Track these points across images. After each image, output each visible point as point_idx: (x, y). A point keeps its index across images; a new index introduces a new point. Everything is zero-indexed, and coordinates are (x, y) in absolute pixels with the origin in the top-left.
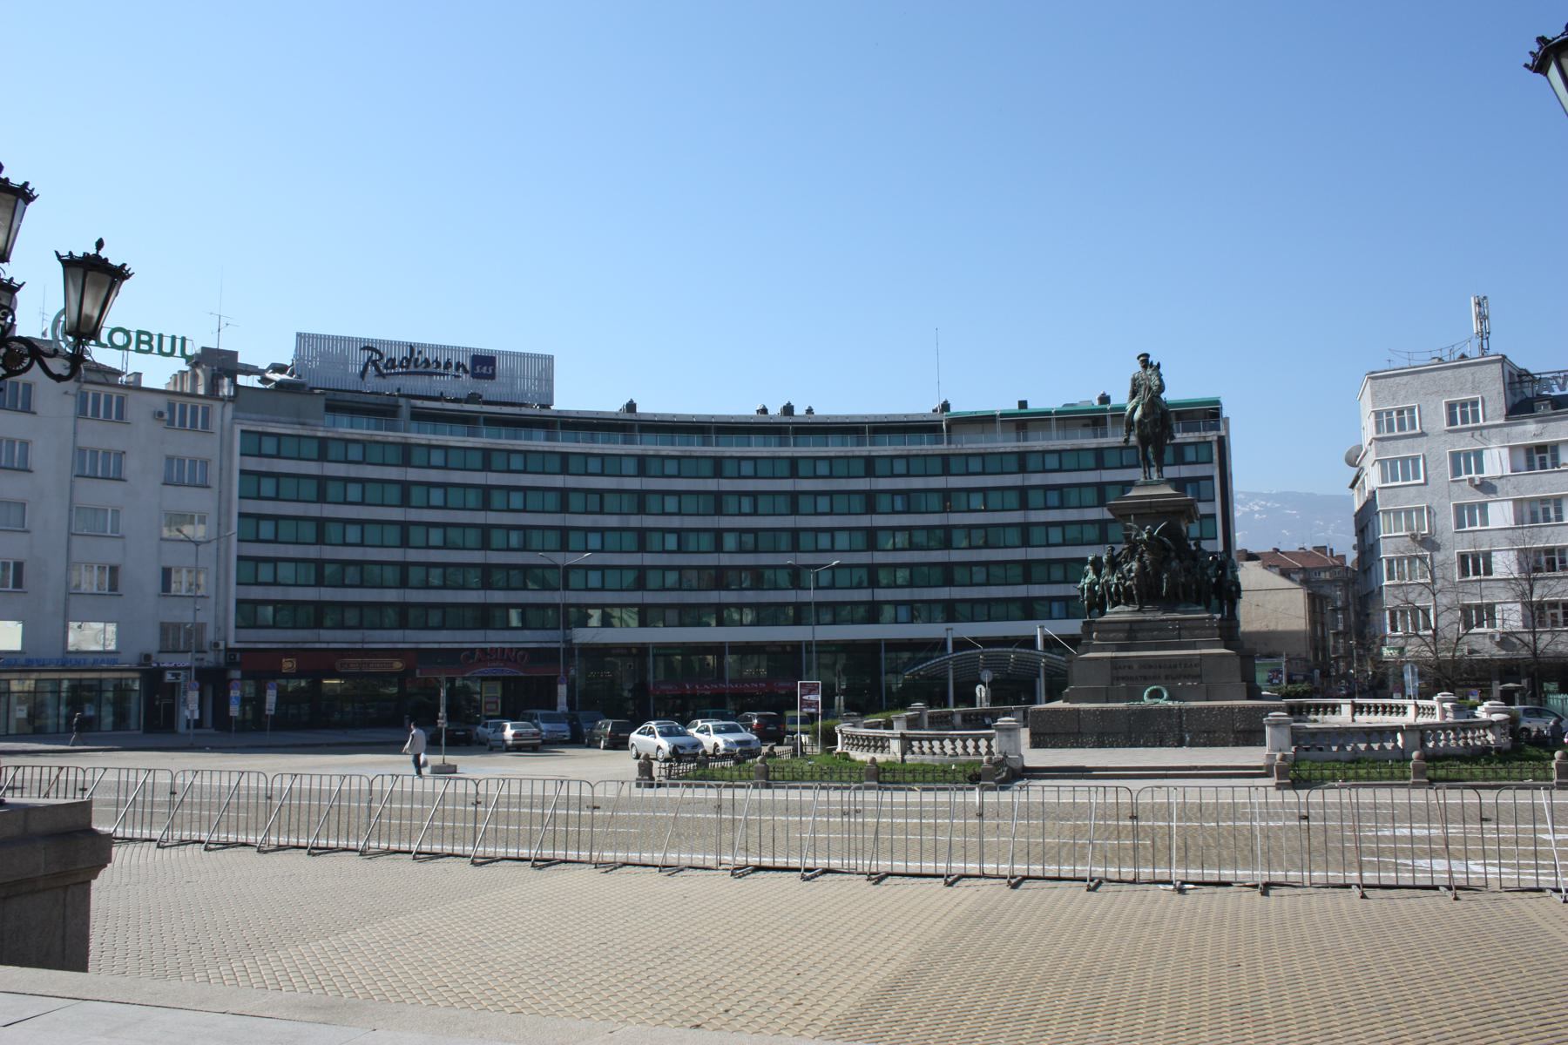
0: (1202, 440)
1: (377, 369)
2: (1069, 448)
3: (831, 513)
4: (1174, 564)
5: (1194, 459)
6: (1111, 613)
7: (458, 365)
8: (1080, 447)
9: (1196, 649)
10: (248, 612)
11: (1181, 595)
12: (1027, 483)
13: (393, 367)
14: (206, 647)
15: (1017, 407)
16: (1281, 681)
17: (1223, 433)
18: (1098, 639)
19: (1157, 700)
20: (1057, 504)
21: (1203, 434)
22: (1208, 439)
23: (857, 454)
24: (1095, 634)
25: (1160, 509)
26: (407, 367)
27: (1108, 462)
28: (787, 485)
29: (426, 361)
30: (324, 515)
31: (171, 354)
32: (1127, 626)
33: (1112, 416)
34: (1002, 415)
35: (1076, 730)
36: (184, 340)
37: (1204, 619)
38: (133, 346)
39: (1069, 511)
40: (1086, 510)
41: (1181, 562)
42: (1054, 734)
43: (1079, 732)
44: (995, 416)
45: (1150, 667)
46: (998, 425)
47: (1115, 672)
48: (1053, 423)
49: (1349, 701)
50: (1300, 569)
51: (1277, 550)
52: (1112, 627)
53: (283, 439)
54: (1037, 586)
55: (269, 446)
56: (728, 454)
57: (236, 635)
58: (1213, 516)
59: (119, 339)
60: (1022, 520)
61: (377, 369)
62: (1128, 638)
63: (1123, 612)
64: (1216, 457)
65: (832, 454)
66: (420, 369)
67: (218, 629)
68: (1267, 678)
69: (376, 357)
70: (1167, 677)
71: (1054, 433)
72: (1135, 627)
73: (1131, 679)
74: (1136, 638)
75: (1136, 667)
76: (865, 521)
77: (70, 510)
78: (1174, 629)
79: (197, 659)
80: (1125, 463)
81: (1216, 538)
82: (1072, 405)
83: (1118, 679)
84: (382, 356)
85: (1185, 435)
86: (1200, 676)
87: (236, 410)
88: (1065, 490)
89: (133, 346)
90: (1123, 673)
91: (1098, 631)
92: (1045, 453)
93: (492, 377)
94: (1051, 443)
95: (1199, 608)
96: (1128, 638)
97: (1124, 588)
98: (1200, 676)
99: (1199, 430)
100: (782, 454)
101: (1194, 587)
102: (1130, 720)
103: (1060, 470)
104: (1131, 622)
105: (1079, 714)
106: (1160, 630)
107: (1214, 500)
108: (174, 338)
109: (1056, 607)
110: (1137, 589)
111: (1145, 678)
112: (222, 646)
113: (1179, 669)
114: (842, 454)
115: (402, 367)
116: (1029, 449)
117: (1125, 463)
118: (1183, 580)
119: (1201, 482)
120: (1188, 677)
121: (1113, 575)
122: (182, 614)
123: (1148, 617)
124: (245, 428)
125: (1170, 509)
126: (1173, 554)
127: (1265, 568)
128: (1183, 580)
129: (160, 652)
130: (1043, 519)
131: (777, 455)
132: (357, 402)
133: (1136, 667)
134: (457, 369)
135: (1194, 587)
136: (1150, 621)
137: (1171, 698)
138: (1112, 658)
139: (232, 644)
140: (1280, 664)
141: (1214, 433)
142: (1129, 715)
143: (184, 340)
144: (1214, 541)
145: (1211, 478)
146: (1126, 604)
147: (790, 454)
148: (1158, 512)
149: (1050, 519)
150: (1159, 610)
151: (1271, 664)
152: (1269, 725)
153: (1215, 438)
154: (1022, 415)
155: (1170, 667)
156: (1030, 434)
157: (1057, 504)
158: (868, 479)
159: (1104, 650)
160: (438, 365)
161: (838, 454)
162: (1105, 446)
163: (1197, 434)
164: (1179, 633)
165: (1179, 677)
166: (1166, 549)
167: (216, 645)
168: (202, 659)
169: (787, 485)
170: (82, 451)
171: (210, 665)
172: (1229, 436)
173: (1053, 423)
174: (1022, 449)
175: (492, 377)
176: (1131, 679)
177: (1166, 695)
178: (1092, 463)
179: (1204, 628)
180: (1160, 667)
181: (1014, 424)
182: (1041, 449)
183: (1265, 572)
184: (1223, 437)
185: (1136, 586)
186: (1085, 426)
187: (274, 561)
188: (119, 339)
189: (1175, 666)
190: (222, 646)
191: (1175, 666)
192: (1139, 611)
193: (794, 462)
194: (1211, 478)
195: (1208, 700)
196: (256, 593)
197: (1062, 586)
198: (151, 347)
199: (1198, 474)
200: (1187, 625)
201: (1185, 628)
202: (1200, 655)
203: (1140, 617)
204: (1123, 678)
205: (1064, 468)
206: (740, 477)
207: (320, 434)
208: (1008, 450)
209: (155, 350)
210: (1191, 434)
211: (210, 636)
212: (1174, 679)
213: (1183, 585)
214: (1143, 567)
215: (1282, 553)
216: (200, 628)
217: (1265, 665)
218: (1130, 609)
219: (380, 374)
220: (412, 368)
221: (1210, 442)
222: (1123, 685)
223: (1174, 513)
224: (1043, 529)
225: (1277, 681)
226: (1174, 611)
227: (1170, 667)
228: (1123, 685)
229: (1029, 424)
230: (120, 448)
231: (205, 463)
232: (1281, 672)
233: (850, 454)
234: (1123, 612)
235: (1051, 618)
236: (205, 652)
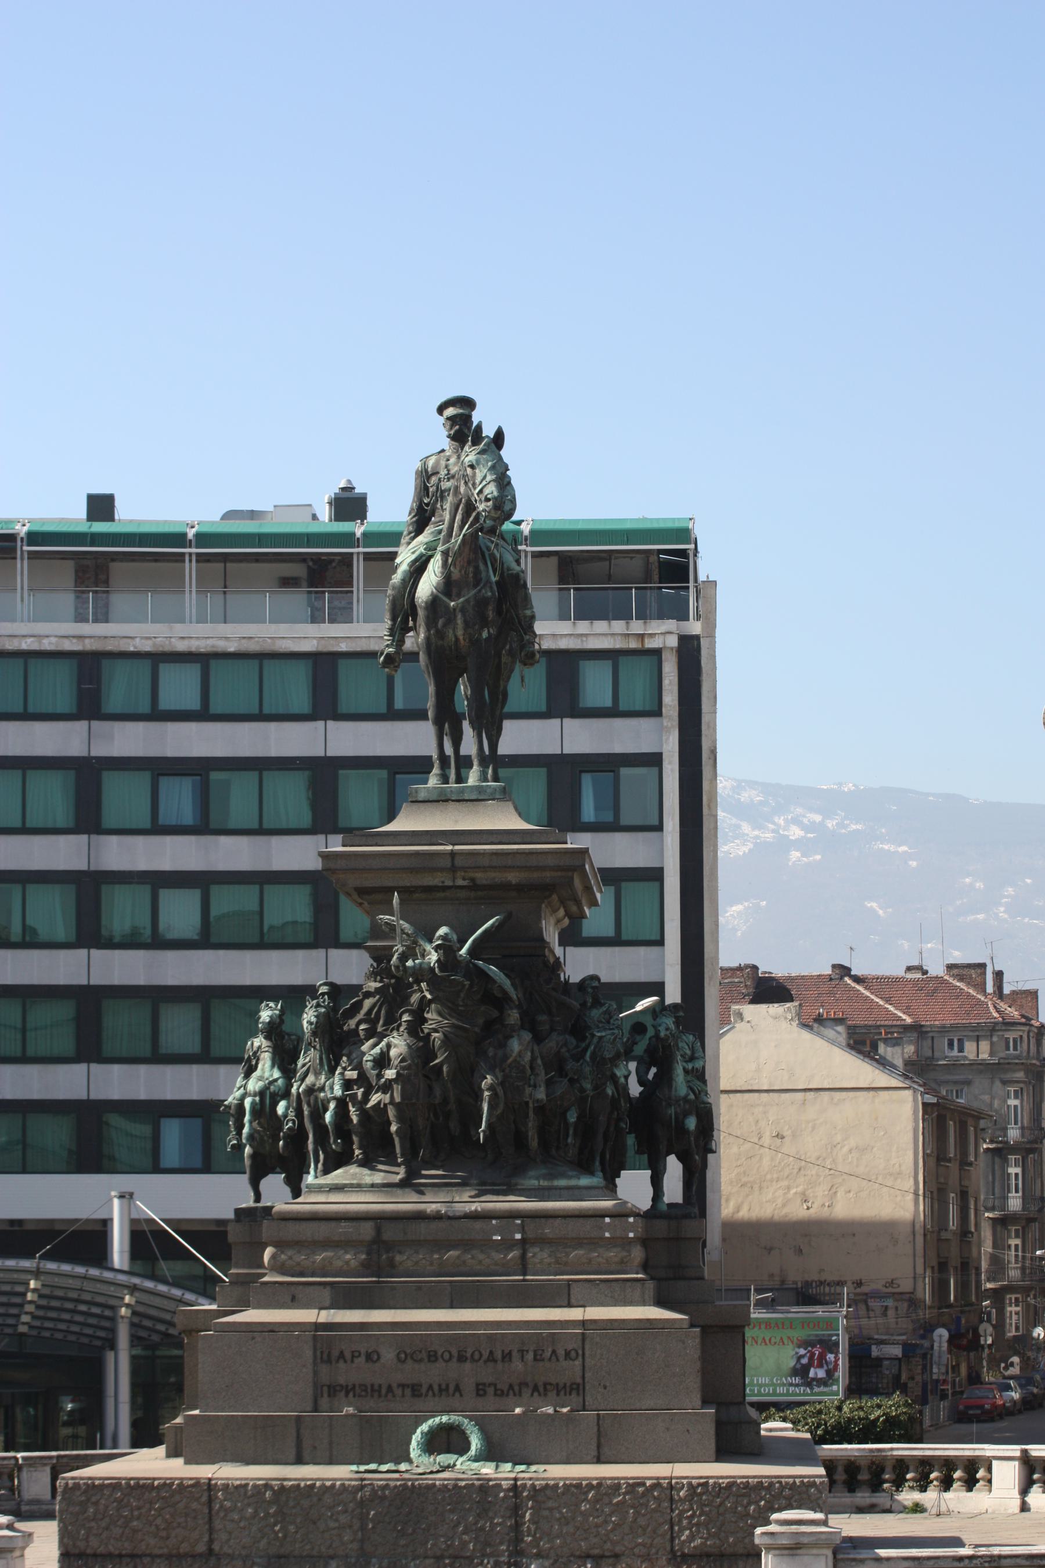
0: (633, 645)
2: (232, 648)
4: (515, 1046)
5: (608, 703)
6: (319, 1189)
8: (269, 647)
9: (570, 1305)
11: (534, 1143)
12: (100, 750)
15: (81, 511)
16: (830, 1373)
17: (694, 627)
18: (282, 1270)
19: (444, 1459)
20: (188, 817)
21: (637, 627)
22: (651, 644)
24: (268, 1253)
25: (481, 877)
27: (349, 697)
32: (367, 1230)
33: (368, 557)
34: (34, 538)
35: (201, 1548)
37: (600, 1215)
39: (225, 841)
40: (275, 840)
41: (538, 1038)
42: (132, 1556)
43: (211, 1551)
44: (12, 538)
45: (433, 1357)
46: (22, 566)
47: (324, 1369)
48: (190, 568)
49: (1015, 1450)
50: (907, 1028)
51: (843, 971)
52: (323, 1230)
54: (116, 1068)
58: (656, 875)
60: (79, 864)
62: (367, 1268)
63: (358, 1187)
64: (670, 699)
68: (792, 1363)
70: (480, 1390)
71: (190, 599)
72: (390, 1233)
73: (371, 1391)
74: (392, 1268)
75: (388, 1355)
78: (508, 1244)
80: (399, 704)
81: (660, 942)
82: (252, 515)
83: (333, 1390)
85: (583, 627)
86: (577, 1388)
88: (215, 776)
90: (345, 1374)
91: (279, 1245)
92: (159, 659)
94: (180, 629)
95: (585, 1181)
96: (367, 1268)
97: (364, 1114)
98: (577, 1388)
99: (625, 615)
101: (572, 1117)
102: (363, 1518)
103: (203, 714)
104: (379, 1219)
105: (210, 1501)
106: (466, 1245)
107: (659, 828)
109: (172, 1131)
110: (400, 1119)
111: (416, 1391)
113: (517, 1365)
116: (110, 646)
117: (399, 704)
118: (541, 1094)
119: (624, 771)
120: (542, 1390)
121: (332, 1071)
123: (433, 1203)
125: (513, 877)
126: (513, 1016)
127: (805, 1026)
128: (541, 1094)
130: (142, 865)
133: (388, 1355)
135: (572, 1117)
136: (437, 1217)
137: (492, 1453)
138: (317, 1326)
140: (831, 1324)
141: (671, 625)
142: (362, 1503)
144: (654, 950)
145: (654, 760)
146: (367, 1163)
148: (474, 886)
149: (166, 864)
150: (464, 1184)
151: (804, 1323)
152: (769, 1548)
153: (673, 642)
154: (95, 539)
155: (491, 1358)
156: (119, 601)
157: (188, 817)
159: (294, 1302)
162: (343, 647)
163: (619, 626)
164: (523, 1256)
165: (512, 1391)
166: (500, 1001)
172: (712, 636)
173: (190, 568)
174: (89, 645)
176: (371, 1391)
177: (473, 1448)
178: (300, 699)
179: (595, 1242)
180: (462, 1359)
181: (70, 565)
182: (147, 647)
183: (806, 1035)
184: (697, 638)
185: (398, 1106)
186: (287, 582)
189: (507, 1356)
191: (507, 1356)
192: (404, 1184)
194: (654, 760)
195: (599, 1460)
197: (195, 1069)
199: (618, 749)
200: (548, 1230)
201: (542, 1241)
202: (583, 1323)
203: (406, 1202)
204: (349, 1390)
205: (215, 708)
208: (48, 645)
210: (601, 626)
212: (500, 1393)
213: (541, 1109)
214: (422, 1050)
215: (858, 980)
217: (791, 1324)
218: (378, 1178)
221: (657, 653)
222: (351, 1410)
223: (520, 888)
224: (144, 893)
225: (821, 1373)
226: (509, 1189)
227: (491, 1358)
228: (351, 1410)
229: (115, 567)
232: (833, 1347)
234: (358, 1187)
235: (157, 1168)
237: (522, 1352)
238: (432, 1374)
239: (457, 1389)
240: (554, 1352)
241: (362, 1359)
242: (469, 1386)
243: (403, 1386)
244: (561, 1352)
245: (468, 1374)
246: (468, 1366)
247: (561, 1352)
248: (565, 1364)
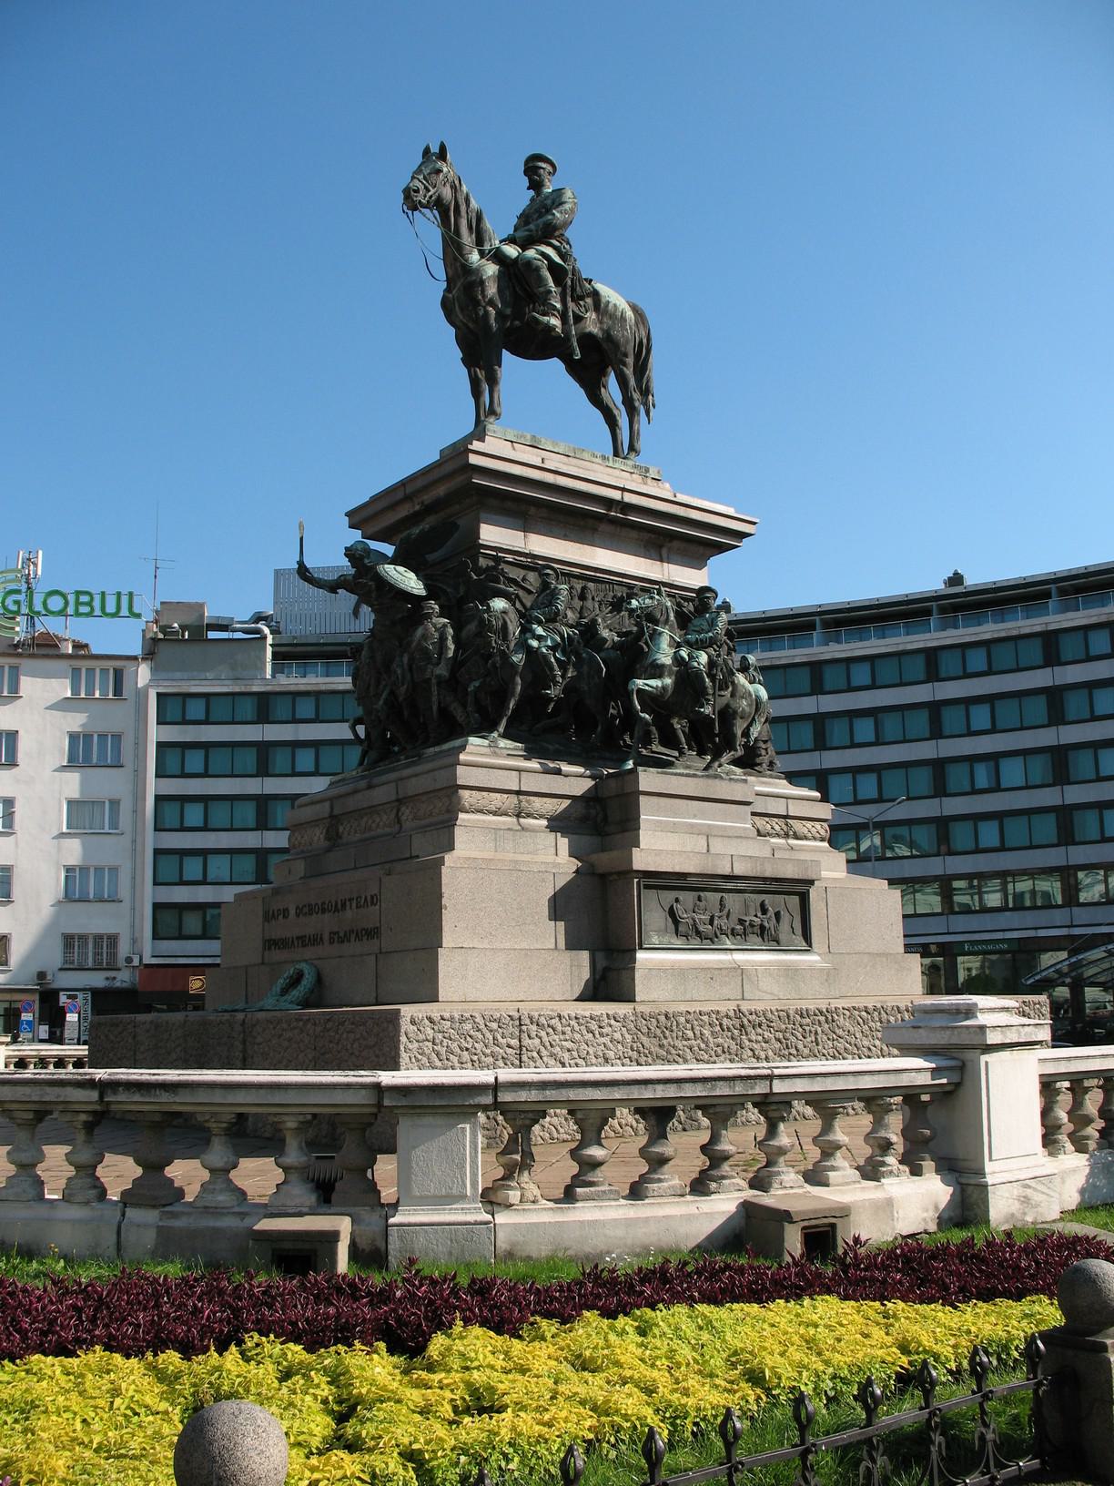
3: (993, 730)
10: (168, 920)
14: (121, 962)
23: (1027, 631)
28: (922, 693)
30: (267, 791)
31: (116, 615)
36: (131, 594)
38: (70, 610)
53: (212, 698)
55: (196, 710)
56: (828, 657)
57: (153, 948)
59: (56, 603)
65: (987, 636)
67: (134, 941)
75: (292, 912)
76: (1047, 737)
79: (107, 979)
87: (154, 670)
89: (70, 610)
100: (910, 647)
108: (119, 594)
112: (136, 962)
114: (1003, 634)
122: (94, 921)
124: (162, 690)
129: (61, 969)
131: (901, 648)
132: (297, 645)
133: (292, 912)
139: (148, 960)
143: (131, 594)
147: (921, 645)
155: (337, 910)
158: (1049, 670)
161: (996, 636)
167: (129, 960)
168: (114, 978)
169: (922, 693)
171: (125, 985)
180: (324, 911)
187: (204, 853)
188: (56, 603)
190: (136, 962)
193: (931, 655)
196: (181, 895)
198: (92, 609)
206: (851, 689)
207: (255, 689)
209: (98, 612)
211: (124, 949)
216: (113, 940)
230: (115, 730)
231: (117, 737)
233: (1015, 633)
236: (119, 970)
237: (350, 900)
238: (311, 925)
239: (321, 939)
240: (366, 899)
241: (281, 917)
242: (326, 937)
243: (298, 938)
244: (369, 898)
245: (324, 924)
246: (327, 916)
247: (369, 898)
248: (372, 908)
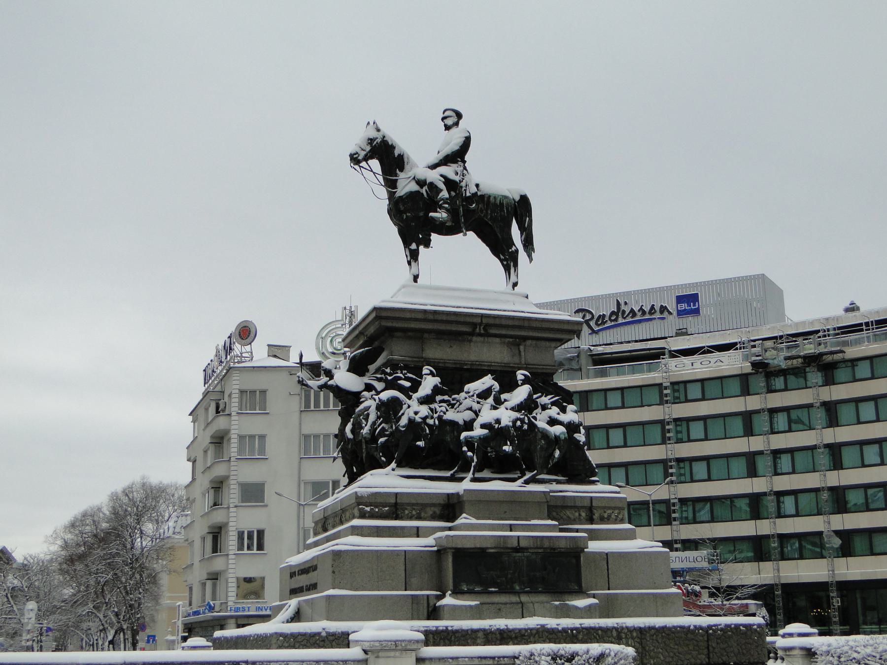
1: (590, 327)
7: (663, 309)
13: (604, 323)
26: (616, 320)
29: (632, 311)
61: (590, 327)
66: (629, 319)
69: (588, 317)
77: (299, 486)
84: (593, 317)
93: (697, 312)
115: (611, 321)
134: (662, 312)
160: (644, 313)
170: (307, 437)
175: (697, 312)
219: (594, 332)
220: (621, 320)
